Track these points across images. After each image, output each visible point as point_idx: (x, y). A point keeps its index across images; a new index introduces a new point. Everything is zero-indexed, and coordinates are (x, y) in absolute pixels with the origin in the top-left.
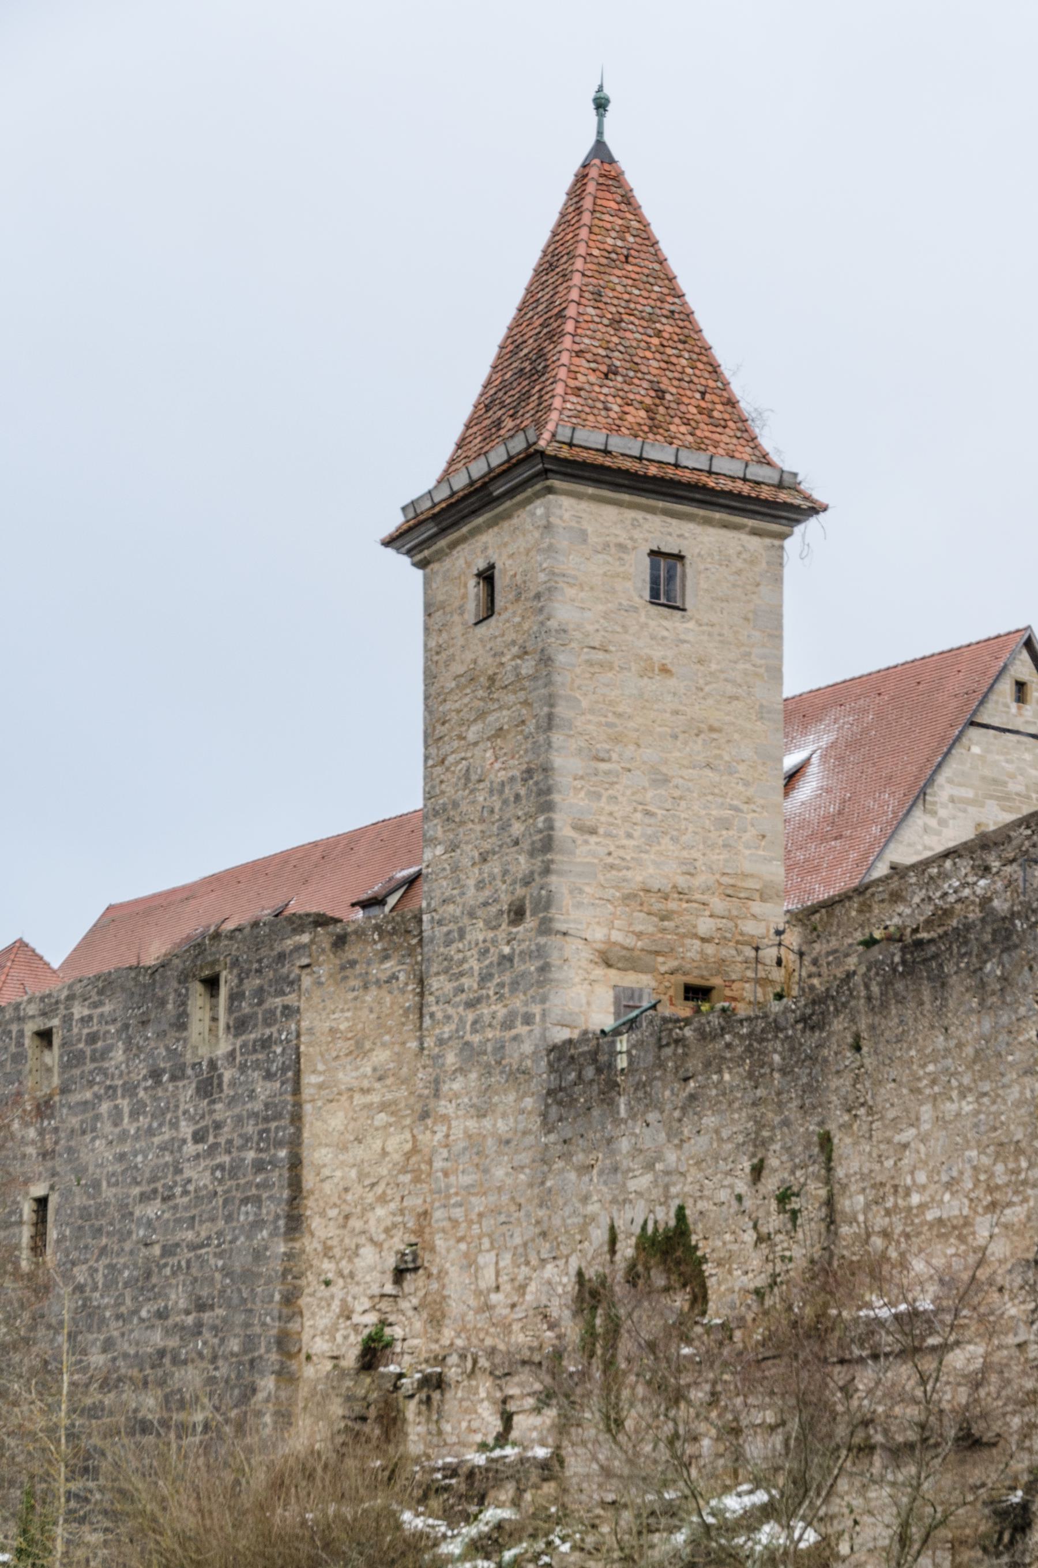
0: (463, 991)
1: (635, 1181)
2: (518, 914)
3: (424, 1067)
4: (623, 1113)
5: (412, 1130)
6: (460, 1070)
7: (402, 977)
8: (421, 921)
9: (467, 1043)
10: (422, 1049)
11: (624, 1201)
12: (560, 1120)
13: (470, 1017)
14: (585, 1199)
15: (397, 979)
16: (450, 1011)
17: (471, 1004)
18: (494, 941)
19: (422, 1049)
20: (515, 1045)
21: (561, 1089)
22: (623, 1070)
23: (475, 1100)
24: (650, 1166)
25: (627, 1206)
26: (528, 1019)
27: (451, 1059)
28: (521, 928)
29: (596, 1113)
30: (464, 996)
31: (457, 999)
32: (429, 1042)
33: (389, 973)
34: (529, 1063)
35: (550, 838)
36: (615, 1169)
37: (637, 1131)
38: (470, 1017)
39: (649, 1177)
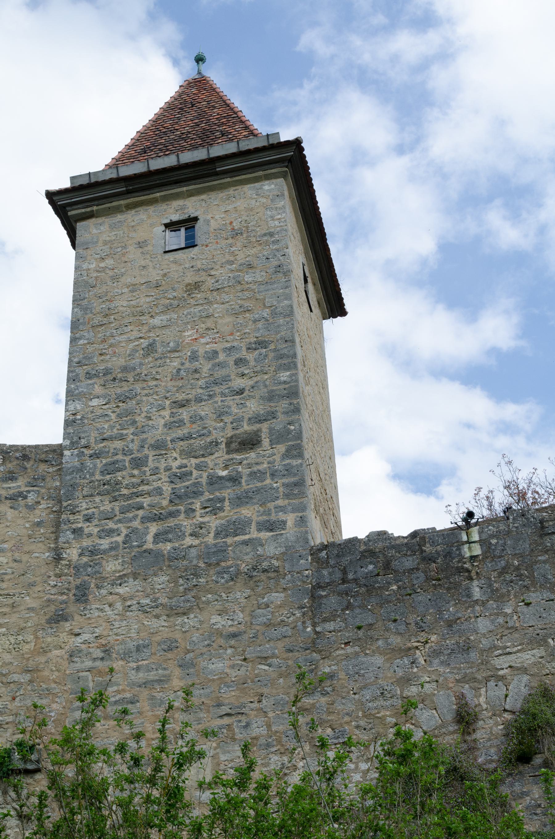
0: (141, 507)
1: (509, 658)
2: (250, 443)
3: (59, 576)
4: (477, 593)
5: (35, 633)
6: (135, 576)
7: (32, 498)
8: (62, 455)
9: (149, 552)
10: (58, 558)
11: (487, 680)
12: (349, 606)
13: (153, 528)
14: (406, 681)
15: (25, 497)
16: (111, 525)
17: (158, 518)
18: (198, 467)
19: (58, 558)
20: (248, 549)
21: (344, 581)
22: (473, 558)
23: (163, 600)
24: (541, 642)
25: (492, 684)
26: (269, 526)
27: (111, 566)
28: (253, 455)
29: (422, 598)
30: (141, 513)
31: (130, 515)
32: (72, 554)
33: (11, 492)
34: (276, 563)
35: (297, 386)
36: (467, 648)
37: (509, 611)
38: (153, 528)
39: (539, 652)
